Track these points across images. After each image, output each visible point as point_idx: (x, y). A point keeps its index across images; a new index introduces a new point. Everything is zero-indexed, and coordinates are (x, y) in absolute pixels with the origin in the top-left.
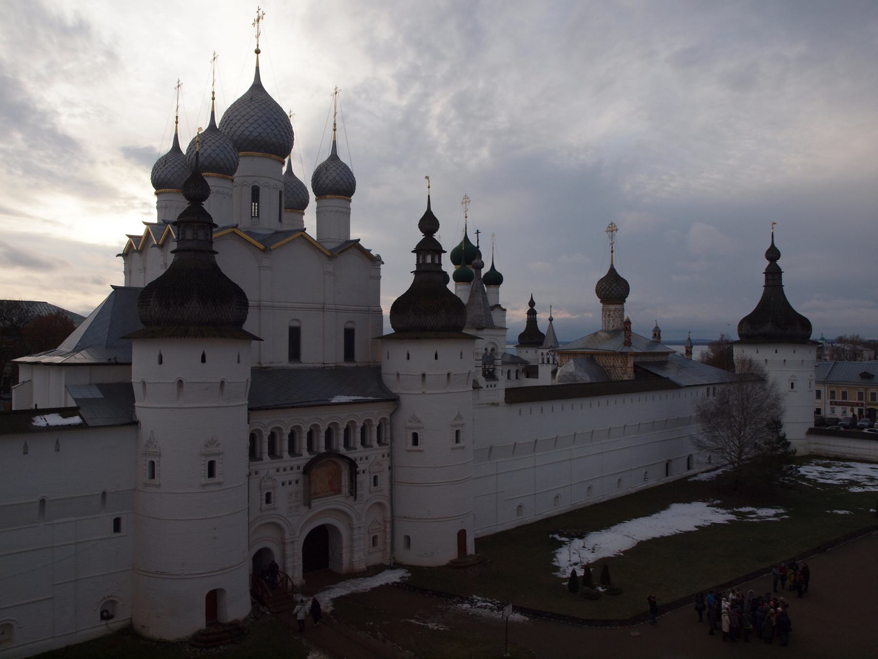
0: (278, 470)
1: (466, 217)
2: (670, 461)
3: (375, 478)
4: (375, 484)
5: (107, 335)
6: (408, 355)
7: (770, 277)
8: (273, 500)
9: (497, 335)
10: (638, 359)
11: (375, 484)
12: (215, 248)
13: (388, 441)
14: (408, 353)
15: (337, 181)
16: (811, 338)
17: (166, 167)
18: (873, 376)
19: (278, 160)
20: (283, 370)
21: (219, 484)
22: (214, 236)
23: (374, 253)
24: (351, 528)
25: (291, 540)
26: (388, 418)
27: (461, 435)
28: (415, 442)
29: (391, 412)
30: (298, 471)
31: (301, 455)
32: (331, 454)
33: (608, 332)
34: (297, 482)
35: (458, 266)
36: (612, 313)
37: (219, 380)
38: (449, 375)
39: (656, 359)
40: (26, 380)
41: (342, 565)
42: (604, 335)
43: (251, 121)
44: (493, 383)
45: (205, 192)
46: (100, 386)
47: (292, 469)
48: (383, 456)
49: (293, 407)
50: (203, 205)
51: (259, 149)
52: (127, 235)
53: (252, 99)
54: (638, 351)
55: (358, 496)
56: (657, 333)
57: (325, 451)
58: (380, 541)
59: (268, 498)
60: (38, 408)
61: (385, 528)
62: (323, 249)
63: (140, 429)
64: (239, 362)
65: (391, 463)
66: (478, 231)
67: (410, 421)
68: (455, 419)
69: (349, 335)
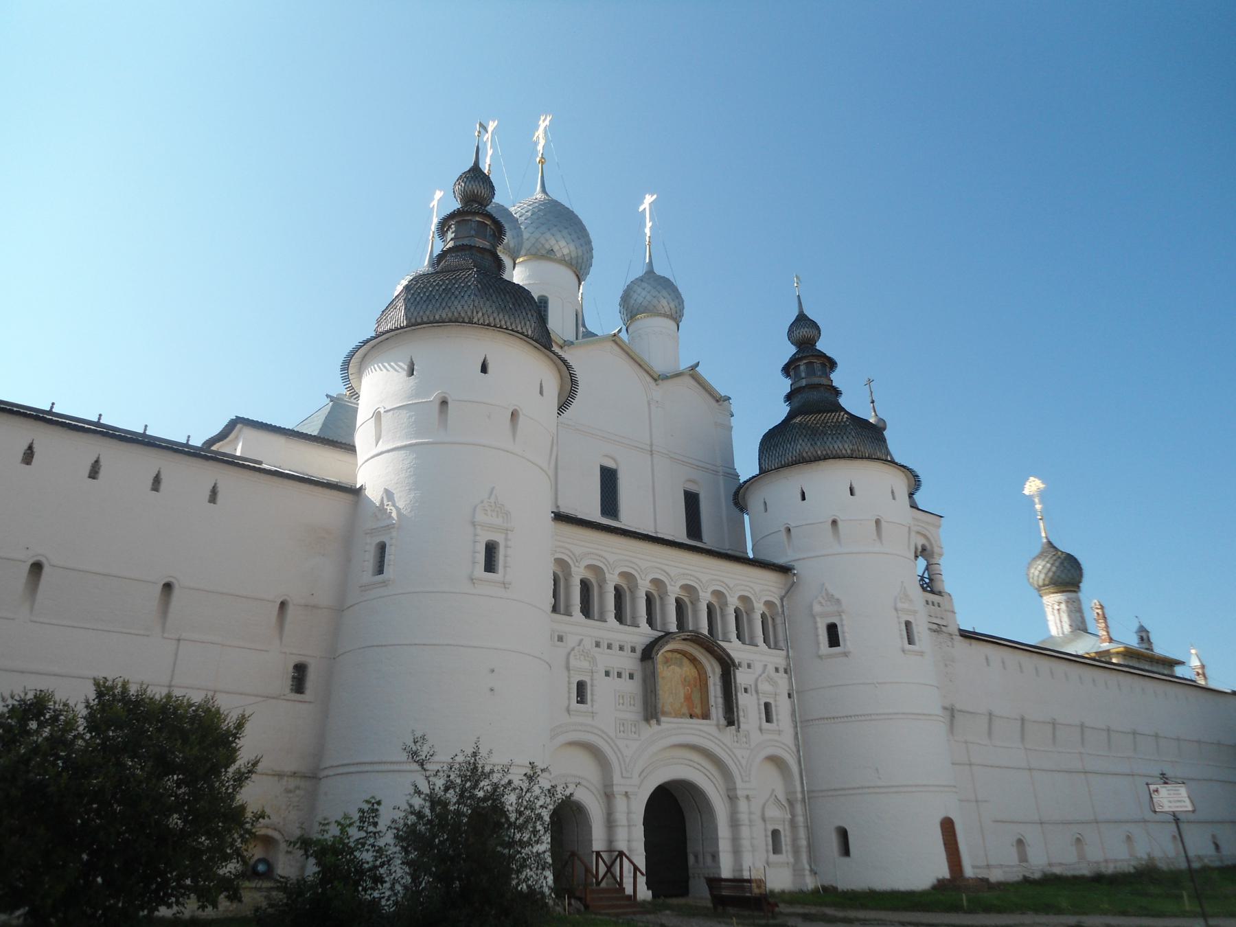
0: (598, 645)
26: (778, 602)
34: (631, 677)
48: (777, 670)
58: (786, 840)
59: (581, 691)
61: (793, 816)
69: (692, 501)
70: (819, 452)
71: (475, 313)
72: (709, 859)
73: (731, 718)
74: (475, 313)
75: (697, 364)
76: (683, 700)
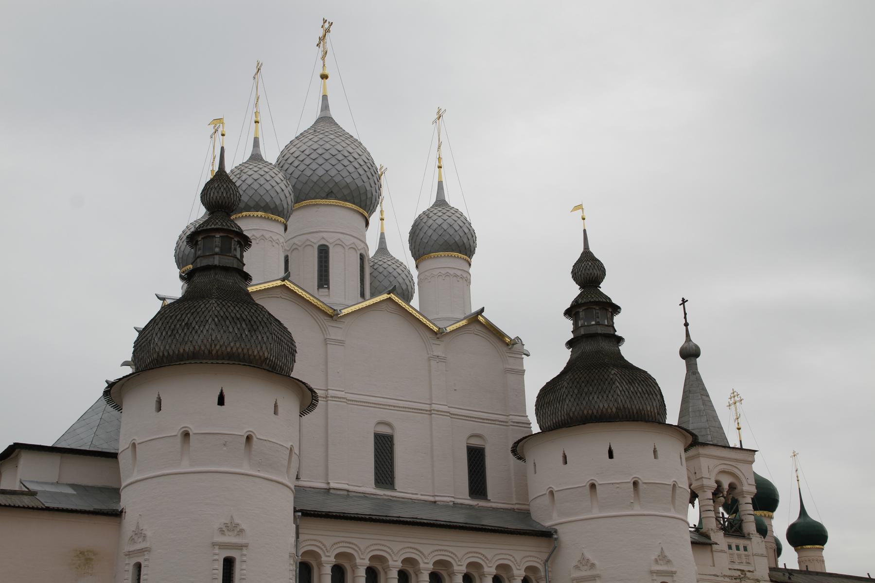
1: (739, 429)
6: (565, 457)
9: (737, 460)
14: (564, 454)
15: (445, 230)
23: (512, 334)
29: (545, 556)
43: (313, 156)
44: (741, 542)
51: (327, 195)
53: (315, 131)
64: (276, 413)
66: (683, 299)
67: (577, 567)
68: (656, 561)
70: (585, 412)
71: (213, 346)
74: (213, 346)
75: (482, 310)
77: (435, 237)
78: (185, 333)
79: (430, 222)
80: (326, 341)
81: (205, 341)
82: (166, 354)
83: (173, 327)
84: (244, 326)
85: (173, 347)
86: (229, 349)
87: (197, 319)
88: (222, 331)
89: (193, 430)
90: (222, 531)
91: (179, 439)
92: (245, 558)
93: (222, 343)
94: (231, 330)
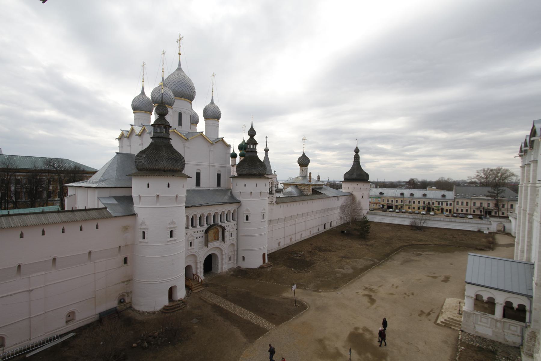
0: (195, 232)
2: (325, 223)
3: (231, 234)
4: (231, 236)
5: (115, 174)
7: (356, 159)
8: (193, 245)
10: (314, 187)
11: (231, 236)
12: (170, 137)
13: (236, 219)
16: (369, 181)
17: (139, 101)
18: (383, 193)
19: (190, 102)
20: (194, 190)
21: (175, 240)
22: (170, 131)
24: (222, 254)
25: (200, 261)
26: (236, 209)
27: (265, 216)
28: (247, 219)
29: (237, 207)
30: (203, 232)
31: (204, 226)
32: (215, 224)
33: (302, 177)
34: (202, 237)
35: (241, 151)
36: (303, 170)
37: (175, 195)
38: (261, 193)
39: (319, 187)
40: (73, 194)
41: (218, 269)
42: (301, 178)
43: (178, 84)
44: (272, 195)
45: (166, 113)
46: (116, 198)
47: (200, 231)
48: (234, 225)
49: (202, 206)
50: (165, 117)
52: (121, 130)
53: (178, 74)
54: (314, 184)
55: (226, 242)
56: (319, 178)
57: (213, 224)
58: (232, 258)
60: (86, 208)
61: (234, 253)
62: (209, 141)
63: (137, 216)
65: (237, 227)
67: (245, 211)
68: (263, 210)
69: (219, 176)
72: (216, 266)
73: (223, 239)
76: (213, 237)
77: (212, 114)
78: (156, 163)
79: (211, 110)
80: (184, 147)
81: (163, 166)
82: (149, 168)
83: (151, 160)
84: (174, 161)
85: (152, 166)
86: (170, 168)
87: (160, 159)
88: (168, 163)
89: (160, 195)
90: (170, 224)
91: (156, 198)
92: (176, 230)
93: (168, 167)
94: (170, 163)
